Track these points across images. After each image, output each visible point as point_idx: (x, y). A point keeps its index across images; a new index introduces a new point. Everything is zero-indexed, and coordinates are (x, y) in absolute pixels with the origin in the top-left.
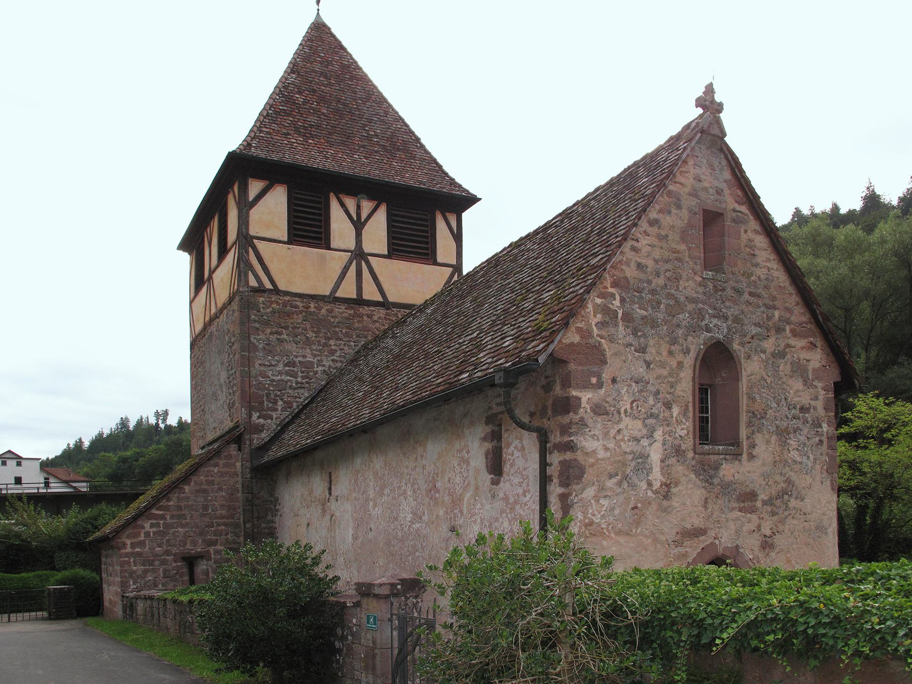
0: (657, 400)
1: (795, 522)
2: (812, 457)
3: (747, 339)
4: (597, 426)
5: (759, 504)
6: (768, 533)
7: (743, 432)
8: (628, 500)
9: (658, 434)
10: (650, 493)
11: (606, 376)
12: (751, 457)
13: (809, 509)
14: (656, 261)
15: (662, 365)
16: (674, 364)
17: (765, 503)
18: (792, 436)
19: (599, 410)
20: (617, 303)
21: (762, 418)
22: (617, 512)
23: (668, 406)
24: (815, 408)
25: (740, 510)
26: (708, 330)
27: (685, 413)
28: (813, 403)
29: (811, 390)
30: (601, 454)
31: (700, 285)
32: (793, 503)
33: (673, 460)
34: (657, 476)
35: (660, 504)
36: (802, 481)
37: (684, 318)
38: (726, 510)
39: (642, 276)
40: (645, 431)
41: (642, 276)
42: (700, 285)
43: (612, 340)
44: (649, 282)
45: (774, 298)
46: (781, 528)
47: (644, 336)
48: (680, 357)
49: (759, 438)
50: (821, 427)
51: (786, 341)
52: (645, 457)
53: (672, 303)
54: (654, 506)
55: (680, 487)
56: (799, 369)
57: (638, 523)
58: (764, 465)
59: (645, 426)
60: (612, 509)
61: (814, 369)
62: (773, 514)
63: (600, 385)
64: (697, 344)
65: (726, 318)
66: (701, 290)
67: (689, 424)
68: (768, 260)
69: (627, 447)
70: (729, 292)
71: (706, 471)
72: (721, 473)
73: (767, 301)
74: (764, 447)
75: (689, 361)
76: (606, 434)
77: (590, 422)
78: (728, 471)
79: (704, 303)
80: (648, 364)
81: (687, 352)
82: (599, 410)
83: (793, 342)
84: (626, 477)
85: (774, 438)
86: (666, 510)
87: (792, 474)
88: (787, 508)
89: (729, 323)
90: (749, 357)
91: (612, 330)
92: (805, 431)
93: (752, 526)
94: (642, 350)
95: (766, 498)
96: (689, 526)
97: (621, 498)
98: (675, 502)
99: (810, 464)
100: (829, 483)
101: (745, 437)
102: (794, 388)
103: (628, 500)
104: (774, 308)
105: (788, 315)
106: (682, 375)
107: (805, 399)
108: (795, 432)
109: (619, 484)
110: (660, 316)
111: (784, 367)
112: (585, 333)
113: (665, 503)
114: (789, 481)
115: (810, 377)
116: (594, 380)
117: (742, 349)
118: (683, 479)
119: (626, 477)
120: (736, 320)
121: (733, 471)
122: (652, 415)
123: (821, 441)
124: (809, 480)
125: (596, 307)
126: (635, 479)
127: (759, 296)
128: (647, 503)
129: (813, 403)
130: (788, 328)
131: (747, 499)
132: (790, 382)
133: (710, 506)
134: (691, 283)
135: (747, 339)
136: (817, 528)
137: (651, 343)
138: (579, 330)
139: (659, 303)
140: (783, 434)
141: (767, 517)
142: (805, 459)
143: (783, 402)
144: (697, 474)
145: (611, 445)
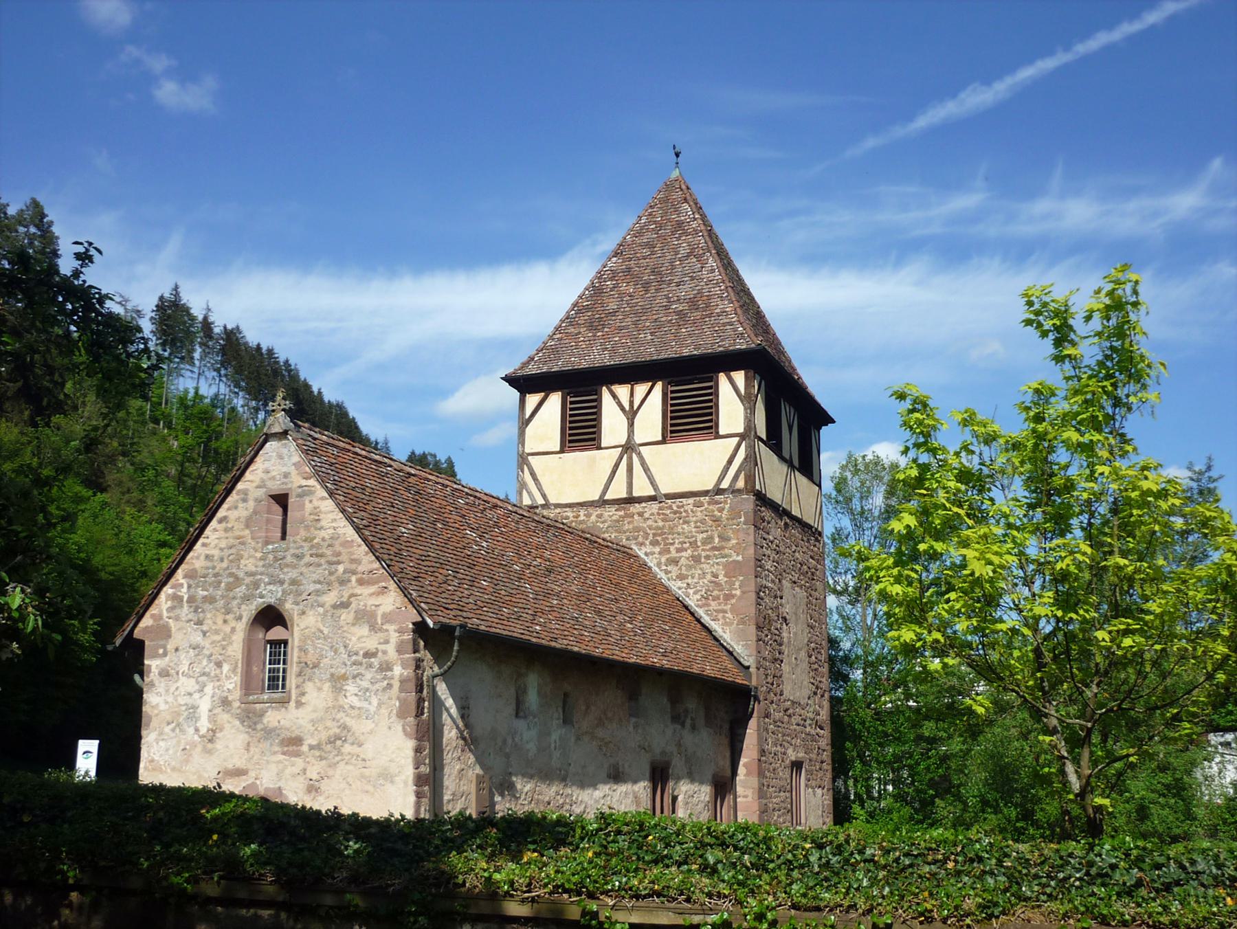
0: (210, 661)
1: (350, 767)
2: (375, 701)
3: (304, 596)
4: (161, 685)
5: (305, 748)
6: (315, 776)
7: (292, 681)
8: (179, 742)
9: (209, 690)
10: (196, 737)
11: (170, 647)
13: (369, 755)
14: (222, 549)
15: (217, 632)
16: (228, 629)
17: (311, 747)
18: (350, 682)
19: (164, 673)
20: (185, 590)
21: (315, 666)
22: (171, 752)
23: (219, 665)
24: (385, 652)
25: (284, 753)
26: (262, 597)
27: (234, 670)
28: (381, 647)
29: (380, 635)
30: (163, 707)
31: (261, 559)
33: (218, 710)
34: (204, 725)
35: (204, 747)
36: (360, 727)
37: (241, 590)
38: (268, 753)
39: (209, 564)
40: (197, 687)
41: (209, 564)
42: (261, 559)
43: (177, 619)
44: (214, 568)
45: (339, 554)
46: (330, 773)
47: (203, 611)
48: (233, 624)
49: (309, 687)
50: (391, 670)
51: (351, 591)
52: (195, 707)
53: (231, 580)
54: (199, 748)
55: (225, 732)
56: (366, 617)
57: (187, 761)
58: (314, 711)
59: (198, 683)
60: (167, 750)
61: (384, 616)
62: (321, 758)
63: (165, 654)
64: (249, 611)
65: (282, 582)
66: (261, 563)
68: (334, 520)
69: (182, 701)
70: (289, 559)
71: (250, 718)
72: (265, 721)
73: (330, 558)
74: (315, 694)
75: (242, 627)
76: (167, 691)
77: (156, 683)
78: (273, 717)
79: (262, 574)
80: (204, 633)
81: (240, 618)
82: (164, 673)
83: (359, 590)
84: (178, 725)
85: (328, 684)
86: (209, 752)
87: (348, 719)
88: (339, 753)
89: (285, 586)
90: (304, 613)
91: (178, 611)
93: (296, 770)
94: (199, 623)
95: (314, 743)
96: (230, 766)
97: (174, 741)
98: (219, 745)
99: (372, 709)
100: (400, 728)
101: (294, 686)
102: (359, 635)
103: (179, 742)
104: (339, 563)
105: (354, 566)
106: (234, 638)
107: (371, 644)
108: (354, 677)
109: (173, 730)
110: (220, 593)
111: (346, 616)
112: (158, 618)
113: (210, 746)
114: (344, 727)
115: (379, 621)
116: (161, 651)
117: (296, 608)
118: (227, 725)
119: (178, 725)
120: (294, 582)
121: (279, 717)
122: (204, 674)
123: (390, 686)
124: (369, 725)
125: (169, 597)
126: (185, 726)
127: (321, 556)
128: (194, 745)
129: (381, 647)
130: (354, 579)
131: (292, 743)
132: (355, 629)
133: (252, 749)
134: (251, 560)
135: (304, 596)
136: (380, 776)
137: (209, 616)
138: (153, 616)
139: (220, 582)
140: (338, 682)
141: (313, 761)
142: (365, 705)
143: (342, 650)
144: (242, 722)
145: (170, 699)
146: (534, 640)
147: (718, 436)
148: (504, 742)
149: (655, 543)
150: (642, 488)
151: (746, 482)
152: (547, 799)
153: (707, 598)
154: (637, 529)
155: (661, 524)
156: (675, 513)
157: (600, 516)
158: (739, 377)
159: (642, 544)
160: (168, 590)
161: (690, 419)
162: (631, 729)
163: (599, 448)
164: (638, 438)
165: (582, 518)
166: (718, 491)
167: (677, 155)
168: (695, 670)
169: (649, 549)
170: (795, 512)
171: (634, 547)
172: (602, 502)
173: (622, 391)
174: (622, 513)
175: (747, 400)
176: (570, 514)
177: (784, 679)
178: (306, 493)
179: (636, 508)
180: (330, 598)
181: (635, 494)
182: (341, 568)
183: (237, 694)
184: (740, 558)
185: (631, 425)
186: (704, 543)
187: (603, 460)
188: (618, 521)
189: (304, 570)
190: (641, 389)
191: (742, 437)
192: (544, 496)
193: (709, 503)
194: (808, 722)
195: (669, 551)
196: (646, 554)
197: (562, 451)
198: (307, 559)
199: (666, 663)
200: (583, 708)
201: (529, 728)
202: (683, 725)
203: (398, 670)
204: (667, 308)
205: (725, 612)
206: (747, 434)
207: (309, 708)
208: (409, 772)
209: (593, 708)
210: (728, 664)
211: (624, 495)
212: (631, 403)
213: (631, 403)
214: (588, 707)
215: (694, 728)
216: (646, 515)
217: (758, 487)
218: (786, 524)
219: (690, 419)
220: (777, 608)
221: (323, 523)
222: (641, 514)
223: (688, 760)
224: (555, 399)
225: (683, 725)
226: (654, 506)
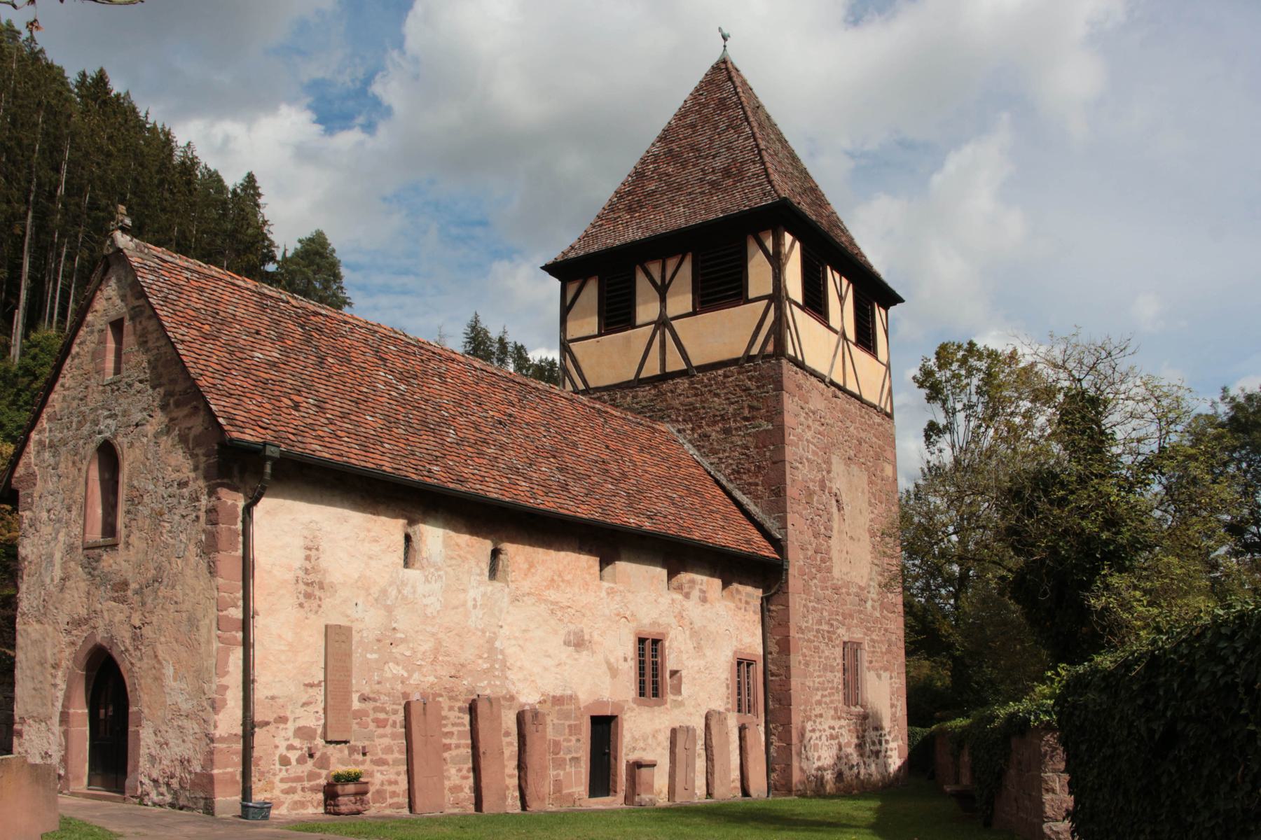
146: (414, 477)
148: (384, 592)
151: (775, 347)
153: (738, 472)
162: (603, 594)
168: (696, 535)
170: (852, 386)
177: (834, 554)
184: (770, 427)
186: (734, 415)
193: (739, 373)
194: (869, 604)
199: (647, 525)
200: (526, 566)
201: (427, 581)
202: (687, 596)
205: (757, 485)
210: (756, 536)
214: (531, 566)
215: (704, 600)
220: (822, 481)
223: (694, 634)
225: (687, 596)
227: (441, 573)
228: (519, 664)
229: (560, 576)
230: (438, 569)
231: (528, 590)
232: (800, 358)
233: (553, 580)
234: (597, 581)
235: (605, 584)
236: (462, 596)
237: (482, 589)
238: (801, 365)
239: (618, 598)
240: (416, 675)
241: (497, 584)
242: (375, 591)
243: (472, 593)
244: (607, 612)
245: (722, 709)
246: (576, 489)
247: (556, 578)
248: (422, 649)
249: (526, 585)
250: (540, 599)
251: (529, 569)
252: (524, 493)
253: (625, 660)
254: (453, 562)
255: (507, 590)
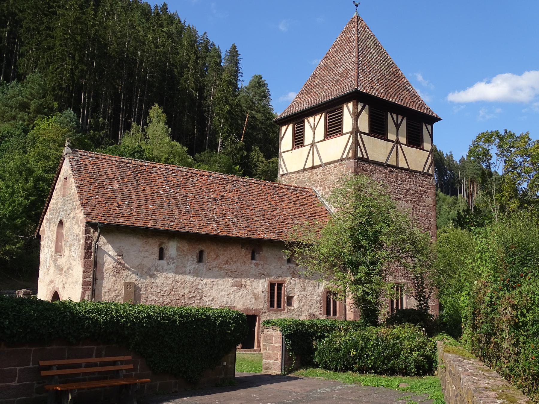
9: (49, 252)
12: (64, 255)
17: (65, 272)
32: (71, 272)
34: (48, 265)
36: (74, 263)
49: (66, 250)
50: (80, 241)
64: (57, 222)
67: (54, 247)
71: (55, 261)
75: (56, 227)
92: (76, 244)
147: (343, 134)
149: (321, 186)
150: (317, 163)
152: (182, 294)
154: (315, 180)
155: (323, 177)
156: (328, 171)
157: (303, 176)
158: (351, 105)
159: (317, 187)
160: (45, 216)
161: (333, 129)
162: (253, 266)
163: (303, 146)
164: (316, 140)
165: (298, 177)
166: (342, 159)
167: (357, 6)
169: (318, 189)
170: (402, 164)
171: (314, 188)
172: (304, 170)
173: (311, 119)
174: (310, 174)
175: (356, 116)
176: (294, 176)
178: (70, 177)
179: (315, 171)
180: (72, 216)
181: (315, 165)
182: (74, 203)
183: (53, 254)
185: (314, 134)
187: (305, 150)
188: (309, 177)
189: (68, 205)
190: (318, 117)
191: (351, 133)
192: (287, 170)
195: (325, 189)
196: (318, 191)
197: (292, 150)
198: (69, 201)
199: (274, 237)
200: (215, 256)
201: (168, 264)
203: (82, 240)
204: (333, 78)
206: (356, 131)
207: (65, 257)
208: (81, 280)
209: (221, 257)
211: (311, 166)
212: (314, 124)
213: (314, 124)
214: (217, 256)
216: (318, 174)
217: (360, 155)
218: (390, 171)
219: (333, 129)
221: (73, 187)
222: (316, 173)
224: (291, 126)
226: (321, 169)
227: (175, 261)
228: (209, 294)
229: (231, 259)
230: (174, 260)
231: (215, 266)
232: (366, 157)
233: (227, 261)
234: (250, 261)
235: (254, 262)
236: (184, 269)
237: (194, 266)
238: (367, 161)
239: (260, 267)
240: (161, 299)
241: (201, 264)
242: (145, 269)
243: (188, 268)
244: (254, 273)
245: (317, 313)
246: (241, 225)
247: (229, 260)
248: (165, 289)
249: (215, 264)
250: (221, 269)
251: (216, 258)
252: (213, 229)
253: (263, 292)
254: (181, 257)
255: (205, 266)
